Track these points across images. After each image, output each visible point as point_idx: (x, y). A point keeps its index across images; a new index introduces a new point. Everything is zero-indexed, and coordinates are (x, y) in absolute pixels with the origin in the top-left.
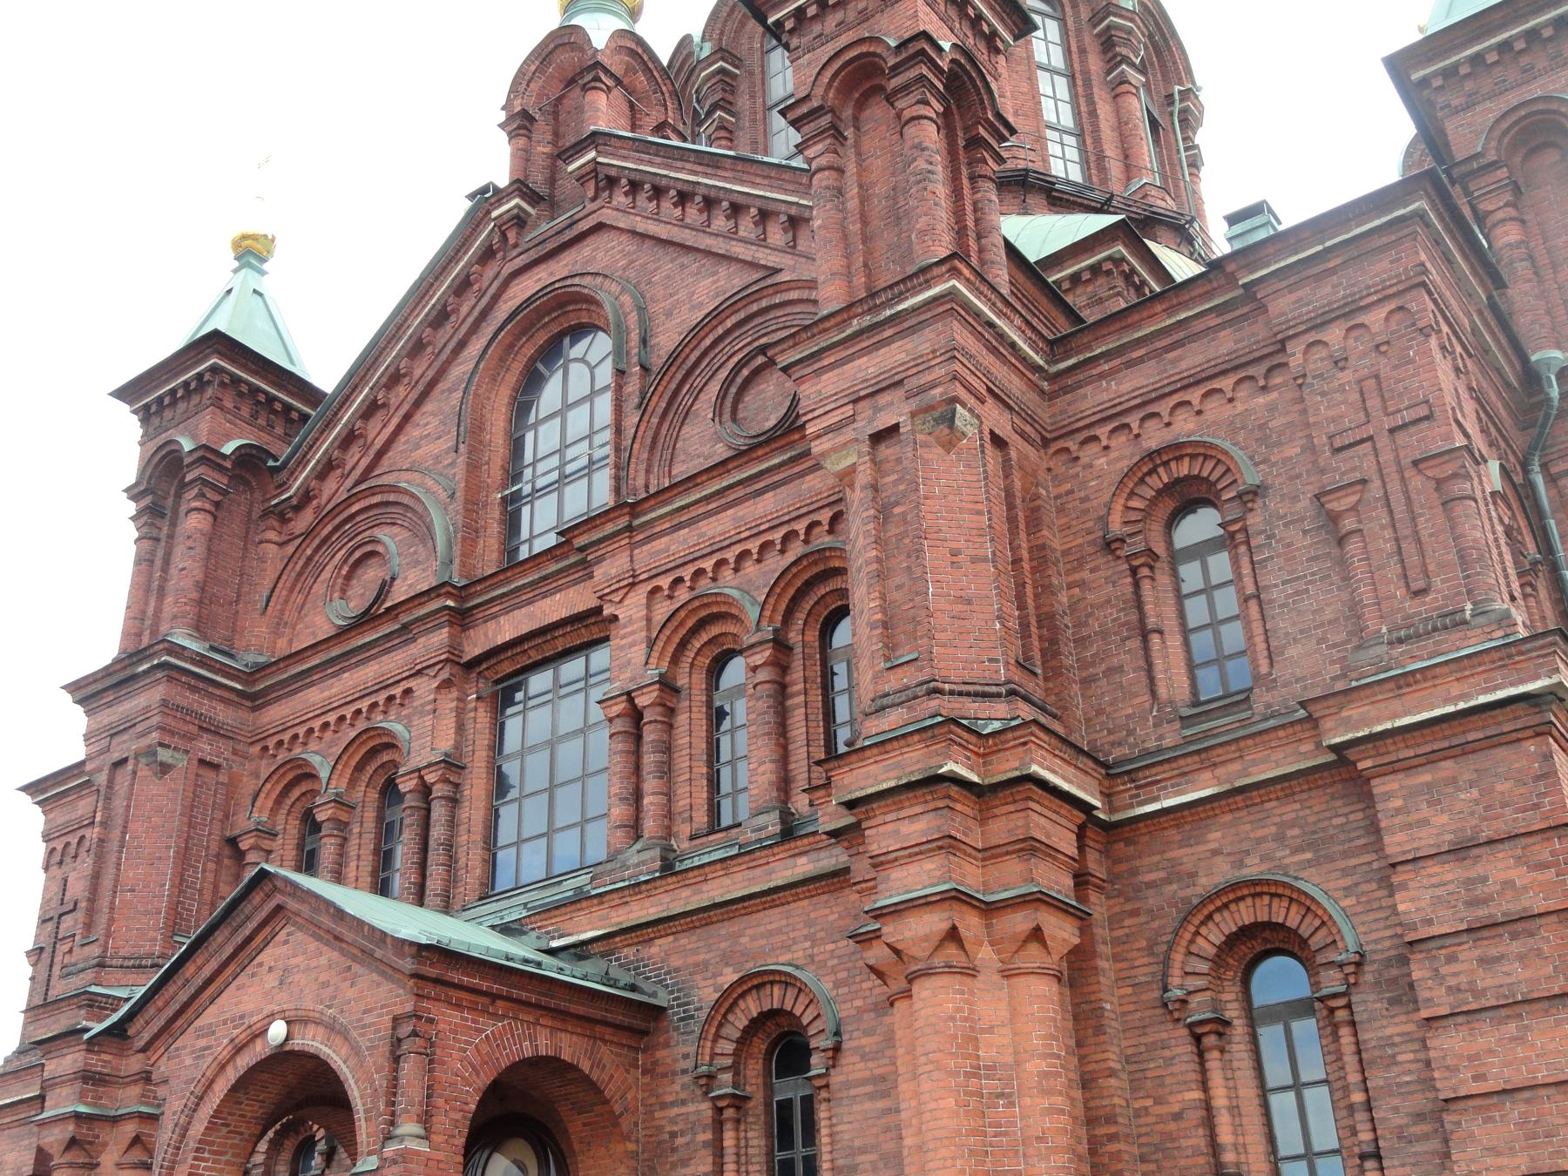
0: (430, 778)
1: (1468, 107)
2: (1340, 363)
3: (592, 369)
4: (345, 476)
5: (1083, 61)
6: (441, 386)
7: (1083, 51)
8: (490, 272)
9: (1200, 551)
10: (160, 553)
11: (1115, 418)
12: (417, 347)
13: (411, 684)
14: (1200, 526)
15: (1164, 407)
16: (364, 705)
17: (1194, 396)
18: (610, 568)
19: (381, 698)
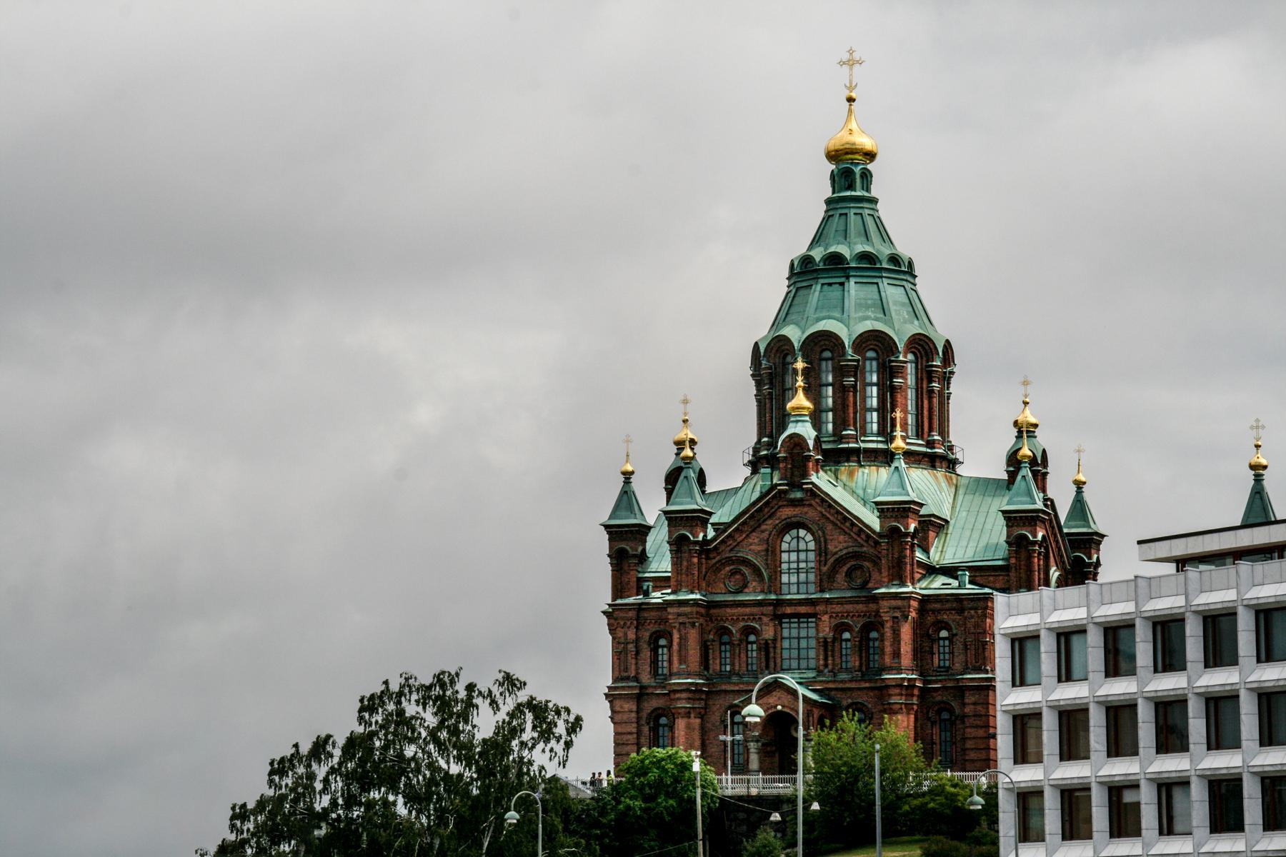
0: (770, 642)
1: (1012, 527)
2: (972, 617)
3: (806, 543)
4: (728, 546)
5: (922, 383)
6: (759, 529)
7: (922, 380)
8: (775, 502)
9: (944, 639)
10: (679, 562)
11: (933, 611)
12: (752, 517)
13: (762, 617)
14: (944, 634)
15: (942, 612)
16: (746, 617)
17: (948, 612)
18: (820, 608)
19: (752, 617)
